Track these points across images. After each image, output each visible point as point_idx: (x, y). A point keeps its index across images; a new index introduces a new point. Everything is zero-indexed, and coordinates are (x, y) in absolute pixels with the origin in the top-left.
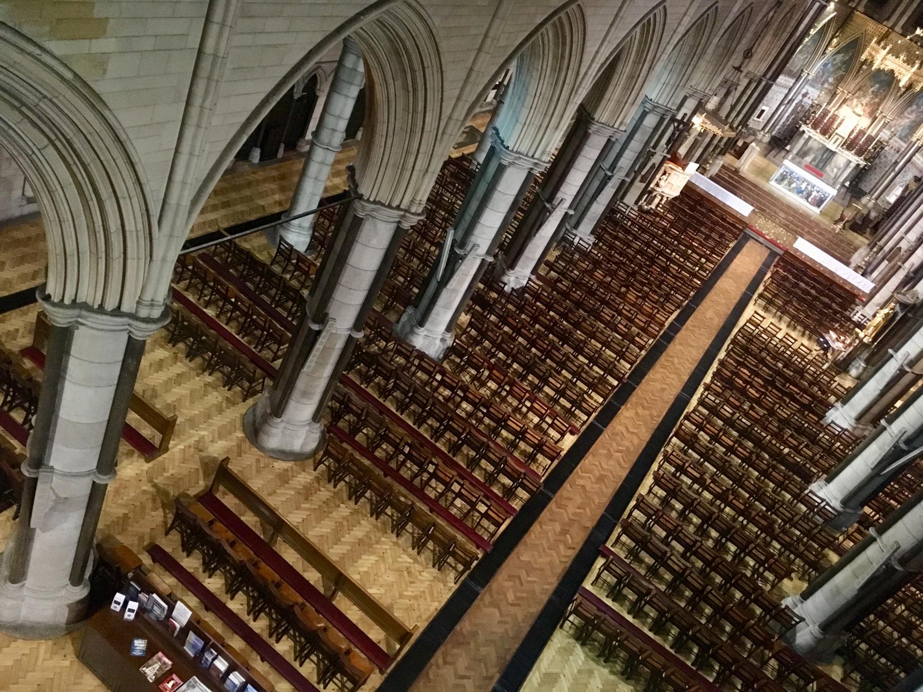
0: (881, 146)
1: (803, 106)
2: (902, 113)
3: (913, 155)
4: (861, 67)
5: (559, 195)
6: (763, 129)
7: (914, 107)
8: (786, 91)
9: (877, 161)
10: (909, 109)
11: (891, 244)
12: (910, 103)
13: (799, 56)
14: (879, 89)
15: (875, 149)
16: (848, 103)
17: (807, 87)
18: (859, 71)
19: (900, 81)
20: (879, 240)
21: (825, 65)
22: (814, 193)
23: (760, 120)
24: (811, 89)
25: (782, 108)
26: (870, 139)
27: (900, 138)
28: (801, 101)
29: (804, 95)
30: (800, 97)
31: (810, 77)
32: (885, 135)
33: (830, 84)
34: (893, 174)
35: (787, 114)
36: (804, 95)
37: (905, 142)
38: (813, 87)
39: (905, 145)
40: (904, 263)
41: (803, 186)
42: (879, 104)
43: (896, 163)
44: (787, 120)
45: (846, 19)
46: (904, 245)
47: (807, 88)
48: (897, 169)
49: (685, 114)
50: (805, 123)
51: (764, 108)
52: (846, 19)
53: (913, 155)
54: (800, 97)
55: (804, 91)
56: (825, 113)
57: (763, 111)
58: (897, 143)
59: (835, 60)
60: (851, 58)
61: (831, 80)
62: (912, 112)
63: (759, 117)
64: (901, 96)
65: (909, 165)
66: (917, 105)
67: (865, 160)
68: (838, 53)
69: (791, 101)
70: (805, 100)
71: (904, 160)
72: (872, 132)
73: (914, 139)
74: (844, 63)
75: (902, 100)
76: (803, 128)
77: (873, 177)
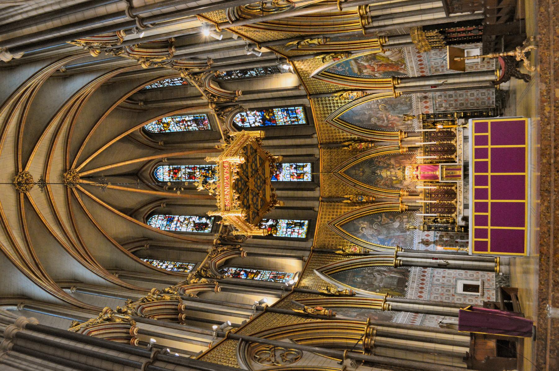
0: (428, 120)
1: (441, 236)
2: (387, 127)
3: (414, 79)
4: (367, 202)
6: (491, 270)
7: (373, 120)
8: (429, 270)
9: (451, 110)
10: (379, 123)
12: (374, 128)
13: (376, 283)
14: (382, 168)
15: (434, 123)
16: (412, 188)
17: (415, 249)
18: (373, 202)
19: (241, 166)
23: (479, 283)
24: (417, 240)
26: (428, 136)
27: (411, 106)
29: (426, 243)
30: (431, 247)
32: (417, 126)
33: (401, 222)
34: (450, 81)
36: (426, 243)
37: (410, 100)
38: (412, 239)
39: (414, 96)
42: (395, 156)
45: (322, 252)
47: (417, 246)
48: (441, 82)
50: (454, 223)
51: (460, 289)
52: (322, 252)
53: (414, 79)
54: (431, 247)
55: (422, 247)
56: (429, 208)
57: (467, 288)
59: (372, 235)
60: (363, 218)
61: (396, 224)
62: (379, 119)
63: (475, 288)
64: (372, 142)
65: (427, 73)
66: (369, 119)
67: (453, 122)
70: (431, 239)
71: (427, 83)
72: (419, 142)
74: (371, 222)
75: (376, 138)
77: (472, 99)
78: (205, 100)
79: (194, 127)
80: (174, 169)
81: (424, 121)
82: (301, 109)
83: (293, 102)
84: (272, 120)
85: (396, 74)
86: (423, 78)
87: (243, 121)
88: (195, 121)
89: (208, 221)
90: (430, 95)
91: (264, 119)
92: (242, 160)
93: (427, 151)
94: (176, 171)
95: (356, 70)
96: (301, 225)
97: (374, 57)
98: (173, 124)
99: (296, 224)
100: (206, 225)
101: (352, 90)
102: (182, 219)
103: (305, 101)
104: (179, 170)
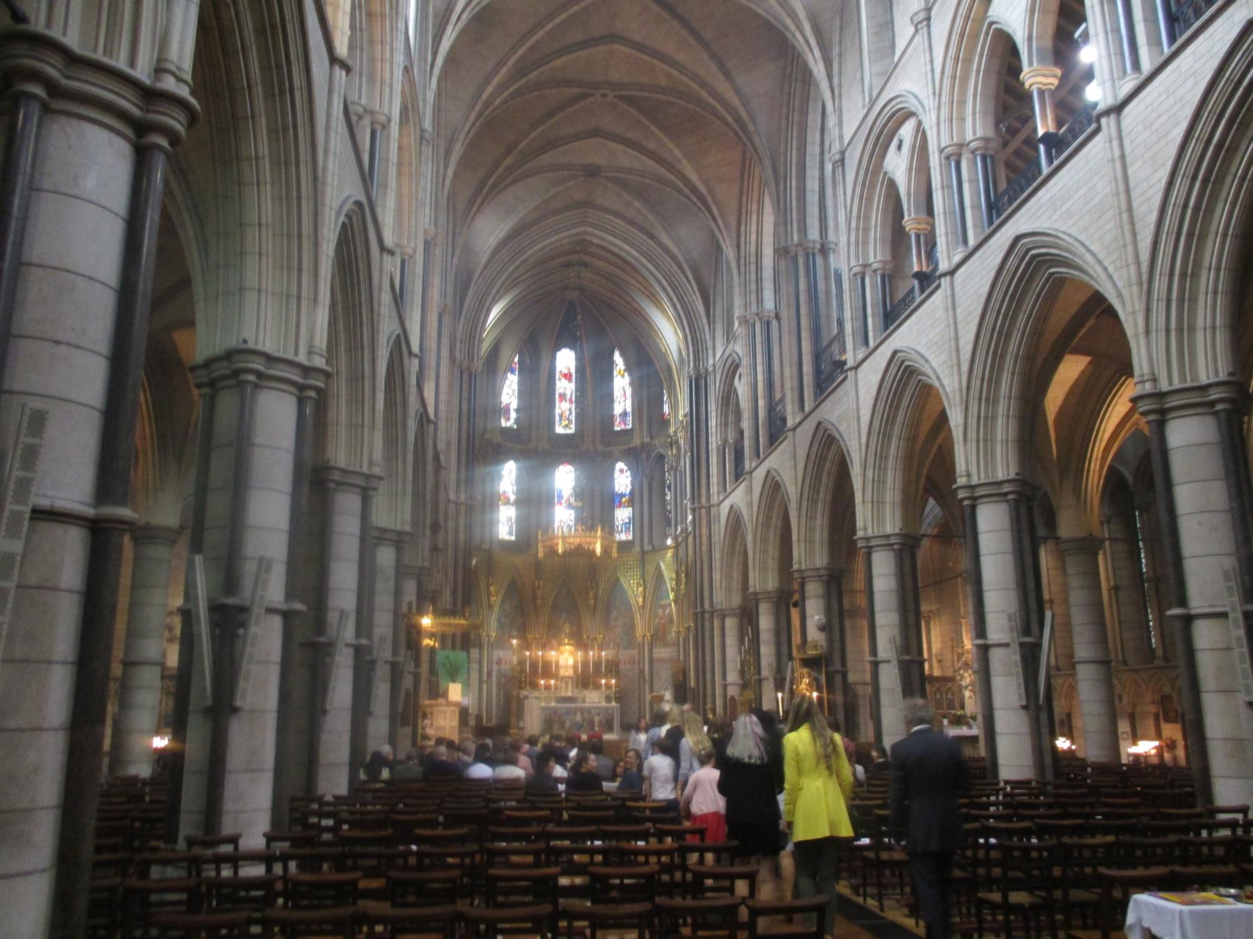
5: (332, 617)
7: (615, 612)
10: (612, 618)
11: (719, 702)
12: (608, 612)
19: (594, 551)
20: (705, 703)
21: (499, 620)
22: (597, 719)
25: (485, 687)
28: (500, 671)
31: (492, 639)
35: (494, 694)
39: (636, 652)
40: (759, 673)
41: (578, 718)
43: (642, 672)
44: (499, 699)
46: (732, 691)
49: (410, 604)
50: (520, 688)
54: (495, 667)
58: (624, 655)
68: (502, 603)
69: (489, 674)
70: (503, 667)
73: (640, 639)
76: (523, 693)
78: (647, 440)
79: (618, 409)
80: (571, 375)
81: (613, 662)
82: (630, 537)
83: (638, 535)
84: (620, 505)
85: (658, 637)
86: (651, 662)
87: (622, 471)
88: (624, 414)
89: (512, 421)
90: (636, 666)
91: (622, 495)
92: (598, 551)
93: (585, 664)
94: (567, 376)
95: (663, 602)
96: (511, 534)
97: (671, 621)
98: (622, 385)
99: (511, 527)
100: (508, 419)
101: (644, 597)
102: (515, 386)
103: (637, 548)
104: (570, 380)
